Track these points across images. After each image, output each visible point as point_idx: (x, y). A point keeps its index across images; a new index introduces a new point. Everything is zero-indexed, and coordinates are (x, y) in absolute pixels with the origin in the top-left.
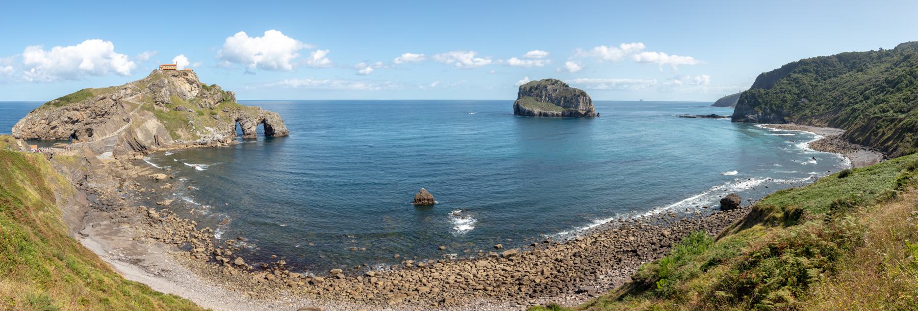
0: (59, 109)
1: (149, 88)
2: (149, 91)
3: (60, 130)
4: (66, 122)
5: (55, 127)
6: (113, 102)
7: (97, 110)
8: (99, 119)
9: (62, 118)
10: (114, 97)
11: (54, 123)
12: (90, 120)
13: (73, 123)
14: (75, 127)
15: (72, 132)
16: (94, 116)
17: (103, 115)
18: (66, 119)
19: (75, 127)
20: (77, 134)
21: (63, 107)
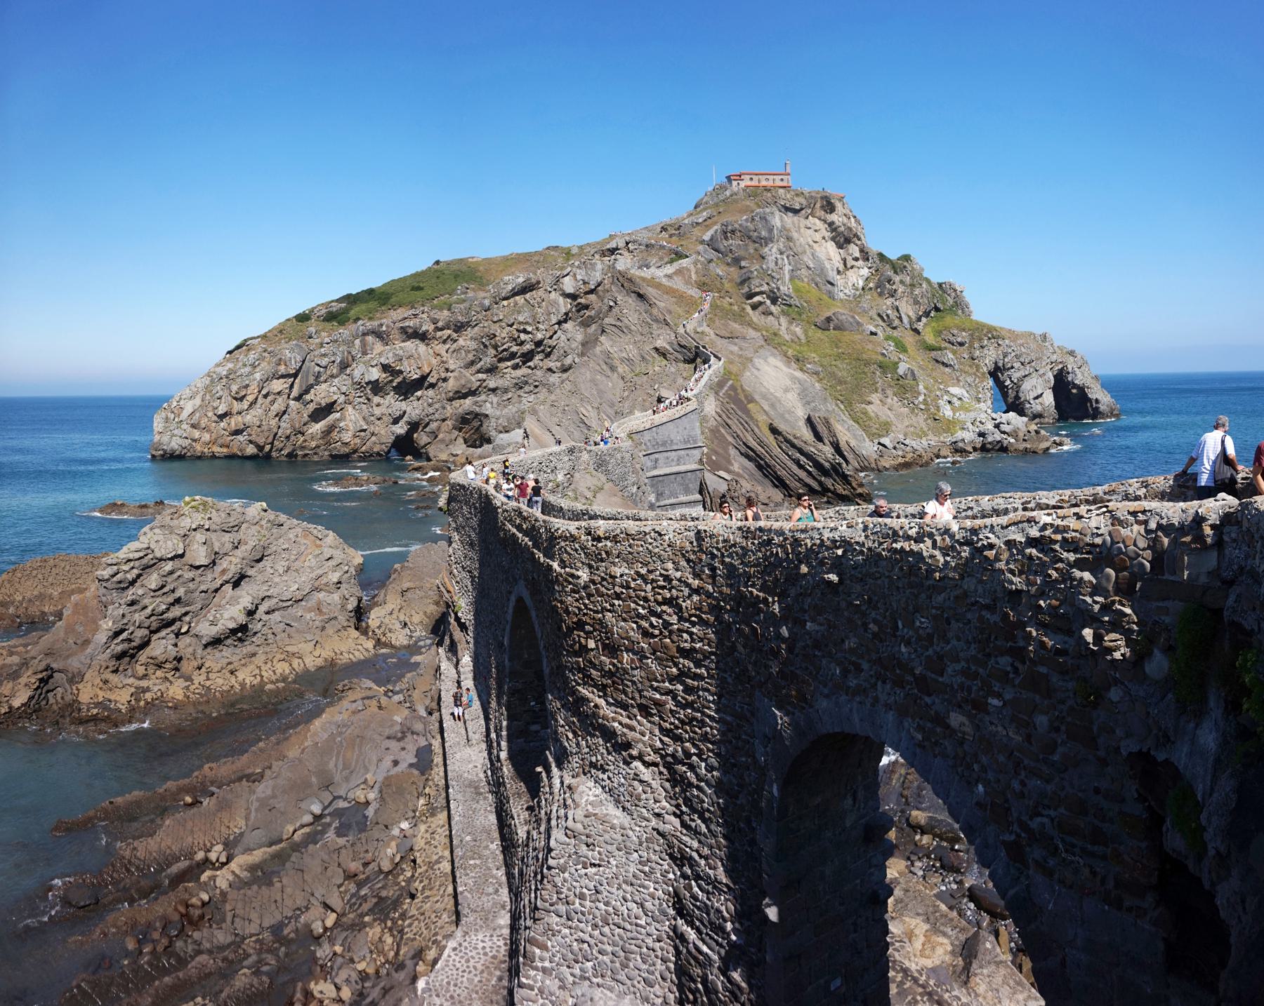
0: (345, 332)
1: (711, 244)
2: (712, 254)
3: (351, 421)
4: (376, 387)
5: (329, 409)
6: (564, 305)
7: (503, 333)
8: (509, 374)
9: (358, 371)
10: (569, 285)
11: (321, 394)
12: (473, 379)
13: (407, 388)
14: (413, 408)
15: (401, 429)
16: (487, 361)
17: (528, 357)
18: (375, 374)
19: (413, 408)
20: (421, 438)
21: (362, 325)
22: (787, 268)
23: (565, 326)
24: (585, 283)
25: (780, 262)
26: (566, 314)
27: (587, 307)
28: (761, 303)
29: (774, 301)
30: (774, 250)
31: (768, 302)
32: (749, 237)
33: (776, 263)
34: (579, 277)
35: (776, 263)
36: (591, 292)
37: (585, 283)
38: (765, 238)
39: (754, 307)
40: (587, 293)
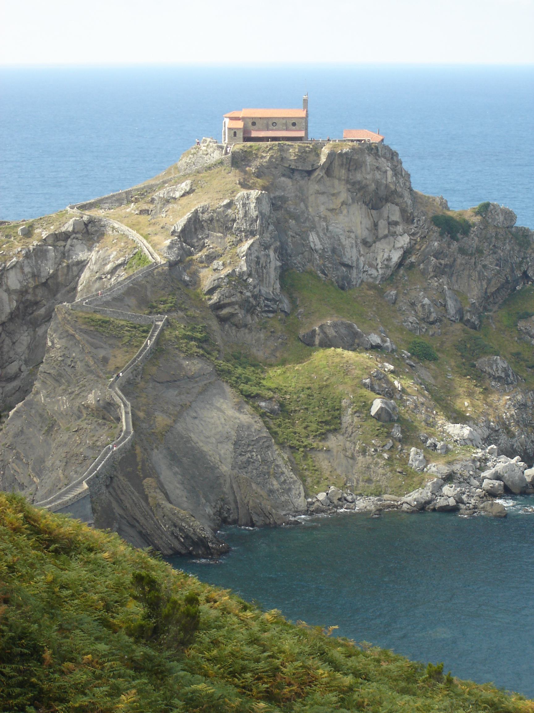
22: (274, 263)
23: (11, 327)
24: (34, 276)
25: (262, 260)
26: (11, 313)
27: (36, 303)
28: (232, 315)
29: (250, 310)
30: (256, 247)
31: (241, 314)
32: (229, 229)
33: (258, 263)
34: (27, 270)
35: (258, 263)
36: (45, 284)
37: (34, 276)
38: (245, 231)
39: (223, 320)
40: (36, 287)
